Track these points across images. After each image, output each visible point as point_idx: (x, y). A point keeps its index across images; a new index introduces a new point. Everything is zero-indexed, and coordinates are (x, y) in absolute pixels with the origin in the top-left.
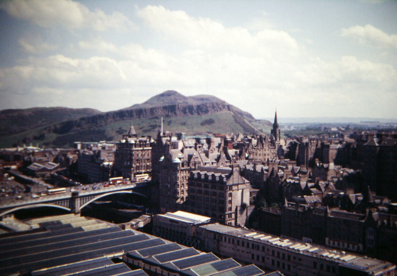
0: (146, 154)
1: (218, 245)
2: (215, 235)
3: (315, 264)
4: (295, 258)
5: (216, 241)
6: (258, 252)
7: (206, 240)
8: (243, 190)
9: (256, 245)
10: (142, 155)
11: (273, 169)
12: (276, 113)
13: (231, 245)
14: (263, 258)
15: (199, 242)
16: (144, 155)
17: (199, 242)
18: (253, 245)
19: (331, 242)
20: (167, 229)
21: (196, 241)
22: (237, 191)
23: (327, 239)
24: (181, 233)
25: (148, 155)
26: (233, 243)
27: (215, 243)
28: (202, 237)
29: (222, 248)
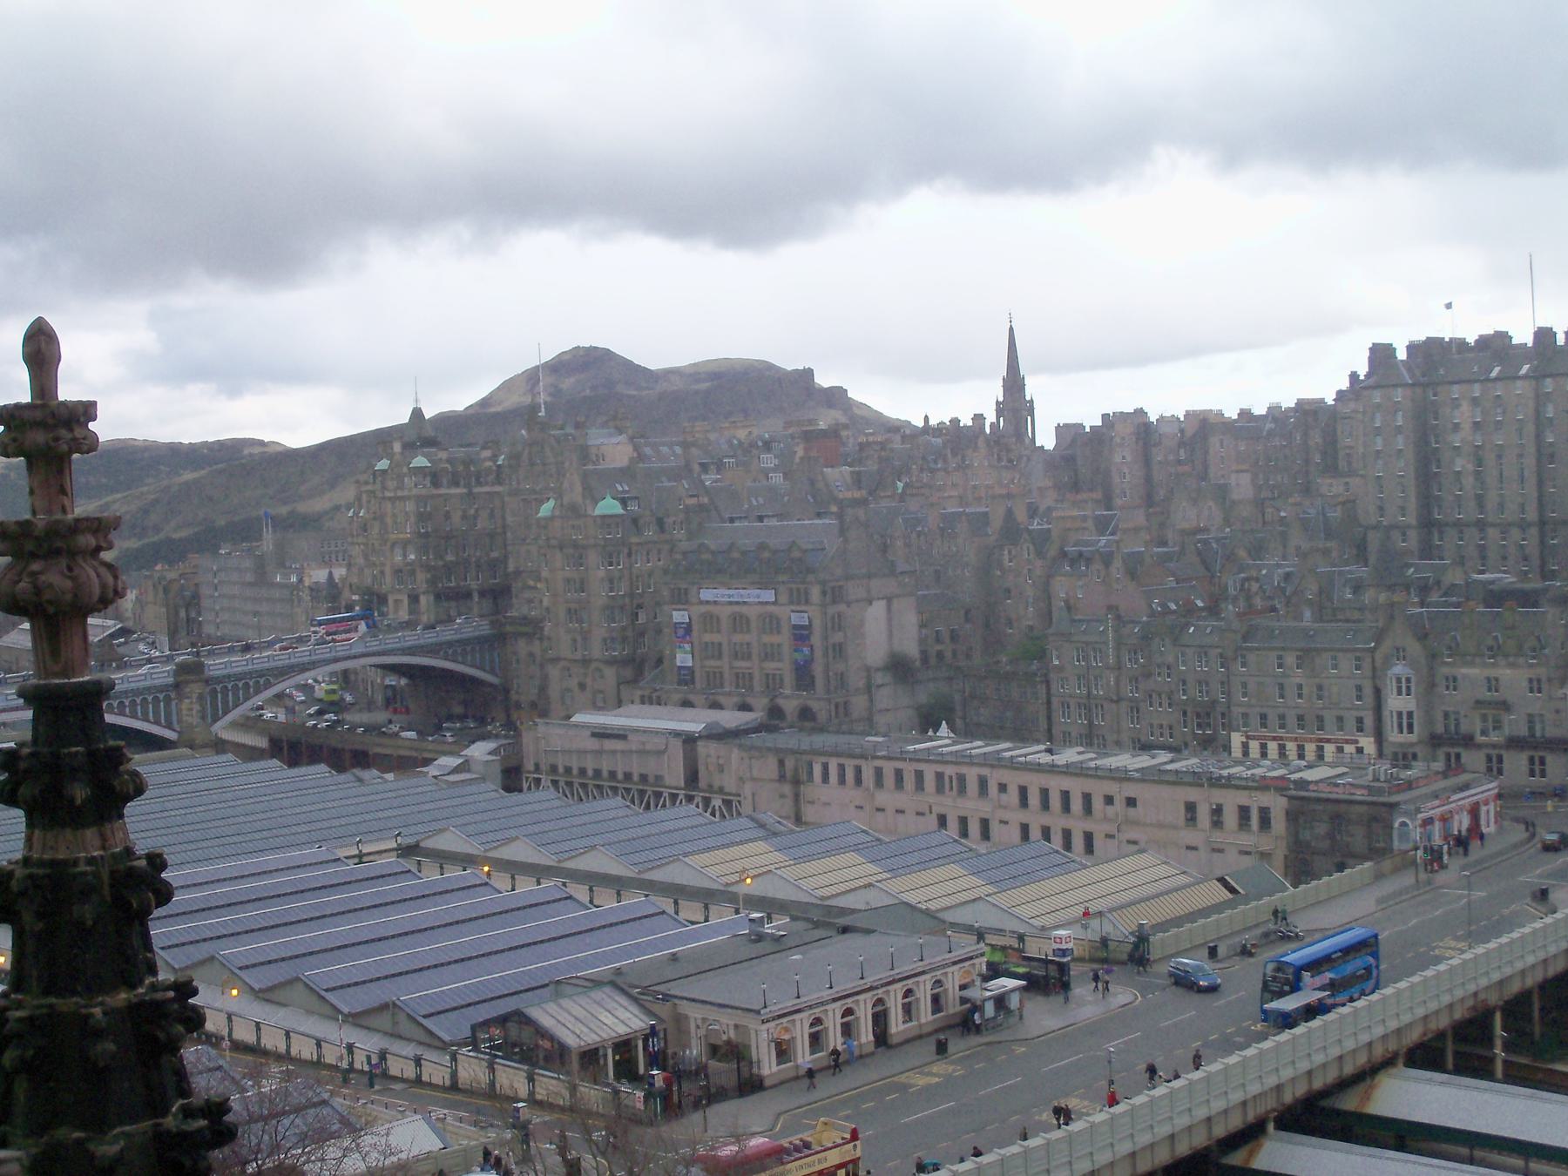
0: (484, 514)
2: (781, 763)
3: (1191, 808)
4: (1109, 800)
5: (787, 789)
7: (747, 790)
8: (889, 600)
10: (464, 517)
12: (1011, 329)
13: (851, 794)
14: (985, 824)
15: (717, 802)
16: (475, 517)
17: (717, 802)
18: (939, 776)
19: (1254, 746)
21: (707, 801)
23: (1237, 739)
24: (644, 778)
25: (492, 515)
26: (859, 781)
27: (782, 796)
28: (730, 784)
29: (809, 813)
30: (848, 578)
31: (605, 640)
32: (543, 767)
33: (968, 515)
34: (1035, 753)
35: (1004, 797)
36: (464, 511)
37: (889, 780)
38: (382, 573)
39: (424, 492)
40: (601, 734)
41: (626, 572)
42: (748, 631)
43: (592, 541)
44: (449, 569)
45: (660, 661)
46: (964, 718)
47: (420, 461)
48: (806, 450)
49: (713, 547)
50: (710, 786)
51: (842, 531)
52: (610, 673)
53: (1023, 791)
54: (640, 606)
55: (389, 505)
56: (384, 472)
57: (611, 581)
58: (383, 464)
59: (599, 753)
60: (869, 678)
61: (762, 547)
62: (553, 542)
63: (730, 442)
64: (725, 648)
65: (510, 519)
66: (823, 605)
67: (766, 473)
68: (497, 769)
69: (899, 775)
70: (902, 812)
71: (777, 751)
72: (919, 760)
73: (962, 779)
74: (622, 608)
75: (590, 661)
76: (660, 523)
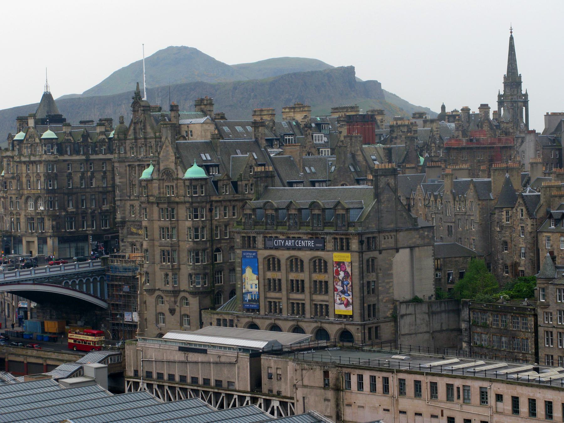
0: (99, 176)
1: (337, 405)
2: (326, 374)
5: (330, 394)
6: (466, 408)
7: (299, 394)
9: (458, 388)
10: (82, 178)
11: (508, 182)
12: (511, 38)
15: (275, 403)
17: (275, 403)
18: (449, 387)
20: (171, 377)
21: (268, 403)
22: (394, 251)
24: (219, 383)
25: (104, 177)
26: (386, 389)
27: (326, 400)
28: (286, 390)
30: (379, 232)
31: (190, 275)
32: (140, 373)
33: (475, 184)
34: (526, 371)
35: (500, 404)
36: (83, 173)
37: (410, 389)
38: (18, 219)
39: (52, 158)
40: (186, 348)
41: (208, 224)
42: (302, 271)
43: (182, 199)
44: (71, 217)
45: (233, 293)
46: (469, 343)
47: (49, 134)
48: (349, 131)
49: (276, 205)
50: (271, 391)
51: (377, 195)
52: (194, 302)
53: (515, 401)
54: (218, 250)
55: (24, 167)
56: (20, 141)
57: (196, 230)
58: (20, 136)
59: (186, 363)
60: (395, 309)
61: (314, 205)
62: (152, 199)
63: (290, 124)
64: (284, 282)
65: (118, 180)
66: (361, 252)
67: (318, 148)
68: (105, 373)
69: (418, 384)
70: (420, 414)
71: (324, 364)
72: (433, 375)
73: (466, 389)
74: (204, 250)
75: (180, 291)
76: (235, 184)
